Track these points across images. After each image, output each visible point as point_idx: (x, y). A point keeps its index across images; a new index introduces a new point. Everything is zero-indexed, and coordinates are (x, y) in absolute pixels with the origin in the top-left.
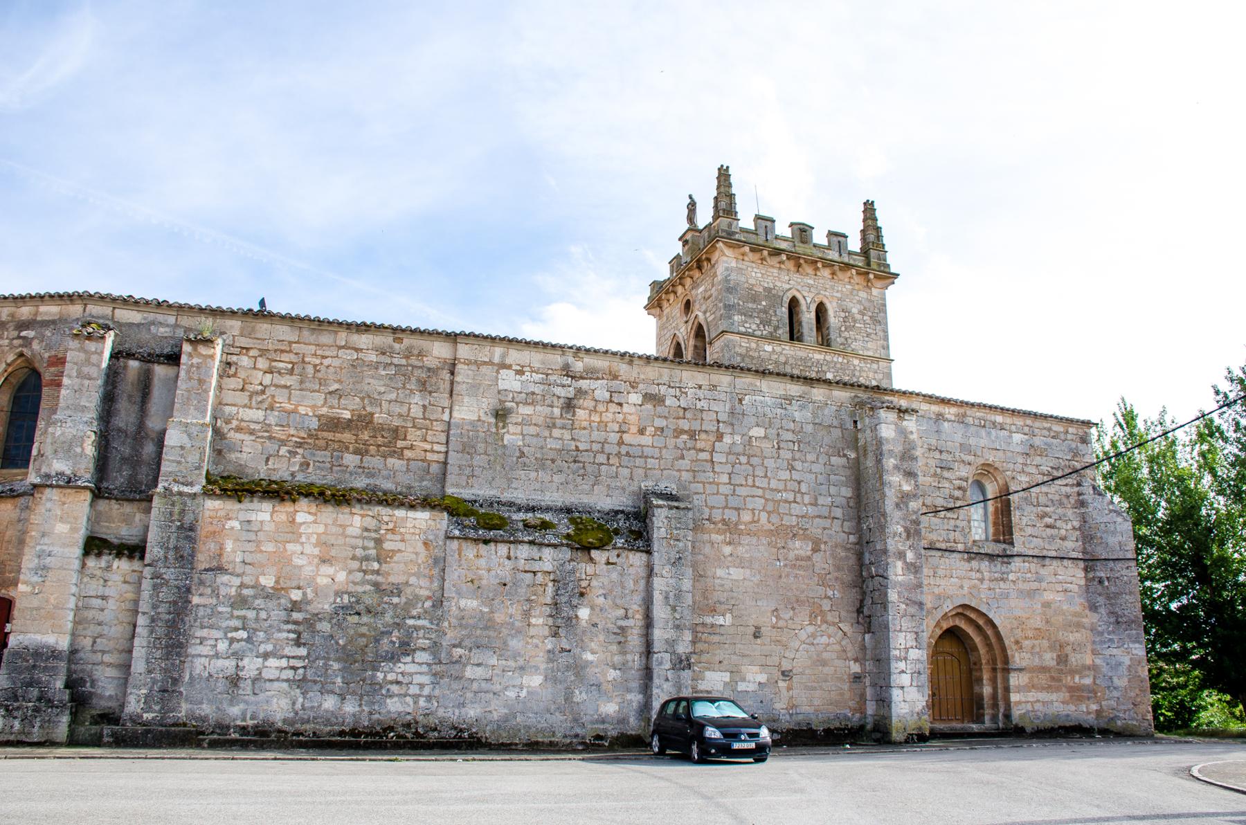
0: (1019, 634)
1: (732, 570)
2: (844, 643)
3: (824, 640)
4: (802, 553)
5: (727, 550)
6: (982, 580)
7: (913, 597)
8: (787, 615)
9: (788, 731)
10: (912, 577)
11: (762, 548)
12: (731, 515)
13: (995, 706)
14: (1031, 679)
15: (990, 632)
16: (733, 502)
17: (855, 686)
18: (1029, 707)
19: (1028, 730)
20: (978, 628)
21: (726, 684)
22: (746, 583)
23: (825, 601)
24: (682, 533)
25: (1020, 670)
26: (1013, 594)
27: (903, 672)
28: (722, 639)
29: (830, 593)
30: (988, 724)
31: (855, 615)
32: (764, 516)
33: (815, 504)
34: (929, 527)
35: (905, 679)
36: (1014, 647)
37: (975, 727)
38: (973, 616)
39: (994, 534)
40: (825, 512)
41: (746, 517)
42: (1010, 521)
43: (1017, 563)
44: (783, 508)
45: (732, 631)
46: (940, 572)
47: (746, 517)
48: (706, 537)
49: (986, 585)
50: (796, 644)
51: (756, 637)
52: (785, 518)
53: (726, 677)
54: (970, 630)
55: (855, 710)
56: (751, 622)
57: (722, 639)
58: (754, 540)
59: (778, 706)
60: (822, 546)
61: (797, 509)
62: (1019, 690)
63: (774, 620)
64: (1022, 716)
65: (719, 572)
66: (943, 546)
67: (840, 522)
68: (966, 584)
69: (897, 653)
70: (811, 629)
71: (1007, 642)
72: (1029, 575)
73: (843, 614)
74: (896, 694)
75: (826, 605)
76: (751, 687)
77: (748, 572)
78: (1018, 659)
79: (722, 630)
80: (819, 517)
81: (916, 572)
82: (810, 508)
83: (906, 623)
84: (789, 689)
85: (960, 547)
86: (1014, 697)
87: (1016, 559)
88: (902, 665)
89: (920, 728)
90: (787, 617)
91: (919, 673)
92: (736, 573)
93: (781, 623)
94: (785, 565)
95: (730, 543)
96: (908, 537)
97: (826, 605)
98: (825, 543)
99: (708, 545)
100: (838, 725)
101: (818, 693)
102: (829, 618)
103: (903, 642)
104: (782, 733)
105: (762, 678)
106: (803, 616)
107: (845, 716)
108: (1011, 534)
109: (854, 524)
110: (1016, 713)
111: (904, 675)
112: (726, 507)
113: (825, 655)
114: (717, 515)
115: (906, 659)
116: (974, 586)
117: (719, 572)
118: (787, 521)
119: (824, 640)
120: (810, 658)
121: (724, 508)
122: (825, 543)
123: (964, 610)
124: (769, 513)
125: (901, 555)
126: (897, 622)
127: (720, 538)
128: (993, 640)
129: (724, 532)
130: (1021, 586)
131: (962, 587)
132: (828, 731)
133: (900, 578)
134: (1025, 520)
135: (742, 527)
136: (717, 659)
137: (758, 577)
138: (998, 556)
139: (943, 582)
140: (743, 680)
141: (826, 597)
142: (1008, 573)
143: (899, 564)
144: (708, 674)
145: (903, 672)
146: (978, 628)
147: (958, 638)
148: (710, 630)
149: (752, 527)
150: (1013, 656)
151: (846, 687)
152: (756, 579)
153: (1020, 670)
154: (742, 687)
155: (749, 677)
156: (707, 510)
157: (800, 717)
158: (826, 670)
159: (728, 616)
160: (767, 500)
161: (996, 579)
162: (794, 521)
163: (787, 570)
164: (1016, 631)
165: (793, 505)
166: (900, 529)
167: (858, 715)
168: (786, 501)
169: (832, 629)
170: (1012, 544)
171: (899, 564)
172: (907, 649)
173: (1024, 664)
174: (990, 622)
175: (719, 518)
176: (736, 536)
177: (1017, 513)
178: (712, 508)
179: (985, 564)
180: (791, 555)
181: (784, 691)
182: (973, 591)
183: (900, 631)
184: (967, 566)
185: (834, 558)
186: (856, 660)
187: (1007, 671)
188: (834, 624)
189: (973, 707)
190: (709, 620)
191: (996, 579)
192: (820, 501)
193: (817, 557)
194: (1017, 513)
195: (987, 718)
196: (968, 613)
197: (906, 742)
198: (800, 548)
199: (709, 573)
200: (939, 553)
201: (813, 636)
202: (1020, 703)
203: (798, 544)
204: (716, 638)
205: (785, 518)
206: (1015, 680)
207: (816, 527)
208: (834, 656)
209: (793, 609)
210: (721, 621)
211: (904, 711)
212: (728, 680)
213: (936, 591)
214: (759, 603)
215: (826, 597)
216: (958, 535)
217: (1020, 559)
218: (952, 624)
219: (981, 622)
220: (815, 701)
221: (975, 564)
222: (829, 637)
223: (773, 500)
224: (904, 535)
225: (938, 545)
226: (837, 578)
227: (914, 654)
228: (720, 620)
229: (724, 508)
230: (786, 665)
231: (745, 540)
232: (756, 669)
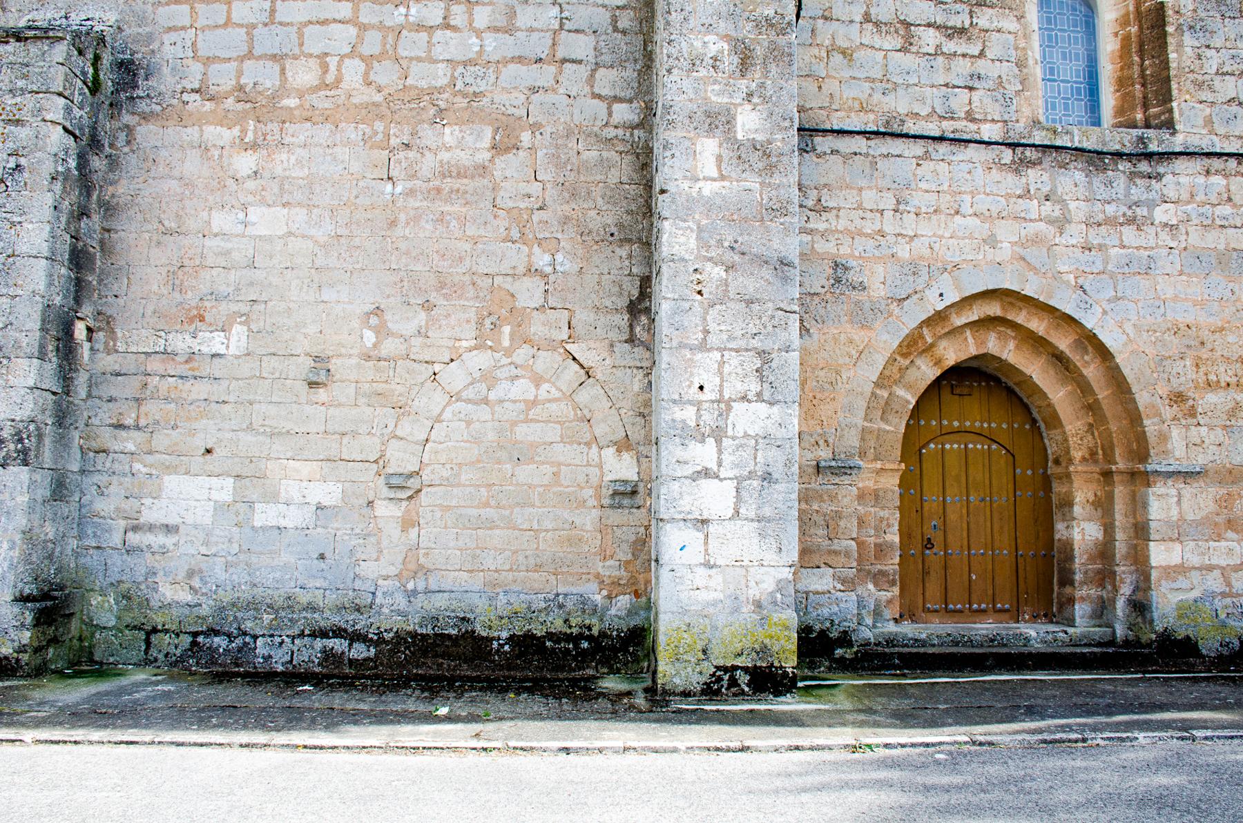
0: (1185, 374)
1: (255, 214)
2: (583, 396)
3: (522, 389)
4: (464, 158)
5: (245, 163)
6: (1061, 223)
7: (754, 241)
8: (407, 322)
9: (400, 639)
10: (753, 182)
11: (342, 152)
12: (262, 75)
13: (1106, 576)
14: (1225, 502)
15: (1091, 371)
16: (267, 41)
17: (616, 517)
18: (1214, 583)
19: (1209, 645)
20: (1037, 343)
21: (221, 508)
22: (295, 244)
23: (527, 282)
24: (29, 101)
25: (1187, 476)
26: (1168, 264)
27: (706, 473)
28: (218, 391)
29: (542, 260)
30: (1082, 624)
31: (623, 319)
32: (353, 71)
33: (509, 30)
34: (885, 79)
35: (716, 498)
36: (1168, 412)
37: (1035, 633)
38: (1038, 325)
39: (1119, 111)
40: (540, 45)
41: (303, 75)
42: (1165, 64)
43: (1183, 178)
44: (412, 45)
45: (246, 368)
46: (919, 200)
47: (303, 75)
48: (192, 133)
49: (1075, 234)
50: (432, 401)
51: (312, 384)
52: (415, 69)
53: (224, 490)
54: (1035, 370)
55: (614, 588)
56: (302, 345)
57: (218, 391)
58: (323, 133)
59: (369, 570)
60: (526, 137)
61: (450, 45)
62: (1178, 534)
63: (370, 337)
64: (1184, 610)
65: (221, 221)
66: (933, 129)
67: (584, 71)
68: (1007, 233)
69: (689, 414)
70: (481, 360)
71: (1142, 399)
72: (1227, 210)
73: (583, 317)
74: (676, 545)
75: (529, 293)
76: (293, 518)
77: (300, 214)
78: (1177, 445)
79: (217, 368)
80: (520, 59)
81: (770, 169)
82: (490, 41)
83: (724, 324)
84: (408, 523)
85: (989, 132)
86: (1160, 555)
87: (1180, 164)
88: (704, 454)
89: (763, 651)
90: (409, 328)
91: (767, 477)
92: (266, 220)
93: (390, 347)
94: (411, 193)
95: (254, 146)
96: (745, 65)
97: (529, 293)
98: (536, 128)
99: (194, 154)
100: (558, 626)
101: (498, 536)
102: (537, 328)
103: (711, 383)
104: (380, 641)
105: (328, 493)
106: (457, 323)
107: (583, 601)
108: (1166, 98)
109: (630, 73)
110: (1167, 603)
111: (707, 485)
112: (250, 55)
113: (522, 431)
114: (222, 77)
115: (718, 434)
116: (1036, 240)
117: (221, 221)
118: (421, 76)
119: (522, 389)
120: (477, 440)
121: (241, 59)
122: (536, 128)
123: (1003, 306)
124: (368, 60)
125: (717, 121)
126: (693, 320)
127: (226, 135)
128: (1103, 393)
129: (241, 119)
130: (1194, 238)
131: (992, 241)
132: (526, 644)
133: (708, 189)
134: (1213, 61)
135: (291, 102)
136: (200, 443)
137: (329, 227)
138: (1118, 155)
139: (925, 228)
140: (272, 497)
141: (531, 271)
142: (1151, 205)
143: (709, 147)
144: (172, 482)
145: (706, 473)
146: (1037, 343)
147: (1010, 391)
148: (182, 369)
149: (321, 101)
150: (1164, 438)
151: (588, 519)
152: (320, 234)
153: (1187, 476)
154: (265, 515)
155: (290, 489)
156: (196, 68)
157: (440, 602)
158: (525, 473)
159: (238, 330)
160: (363, 28)
161: (1110, 222)
162: (441, 76)
163: (413, 203)
164: (1178, 367)
165: (438, 35)
166: (715, 45)
167: (624, 601)
168: (419, 27)
169: (546, 361)
170: (1169, 125)
171: (709, 147)
172: (724, 405)
173: (1200, 460)
174: (1091, 342)
175: (227, 83)
176: (275, 127)
177: (1188, 40)
178: (209, 61)
179: (1072, 181)
180: (428, 164)
181: (392, 531)
182: (1032, 254)
183: (703, 347)
184: (1011, 182)
185: (560, 166)
186: (624, 445)
187: (1140, 478)
188: (552, 345)
189: (1043, 578)
190: (181, 342)
191: (1110, 222)
192: (525, 18)
193: (510, 167)
194: (1188, 40)
195: (1081, 611)
196: (1021, 318)
197: (710, 691)
198: (461, 143)
199: (191, 224)
200: (918, 148)
201: (489, 378)
202: (1181, 570)
203: (450, 135)
204: (199, 390)
205: (415, 69)
206: (1162, 504)
207: (507, 90)
208: (553, 433)
209: (428, 306)
210: (216, 342)
211: (703, 596)
212: (226, 496)
213: (903, 251)
214: (327, 295)
215: (531, 271)
216: (981, 100)
217: (1198, 165)
218: (973, 351)
219: (1063, 343)
220: (482, 558)
221: (1036, 178)
222: (538, 381)
223: (381, 27)
224: (730, 62)
225: (911, 127)
226: (565, 220)
227: (749, 419)
228: (216, 342)
229: (241, 59)
230: (401, 459)
231: (299, 133)
232: (306, 469)
